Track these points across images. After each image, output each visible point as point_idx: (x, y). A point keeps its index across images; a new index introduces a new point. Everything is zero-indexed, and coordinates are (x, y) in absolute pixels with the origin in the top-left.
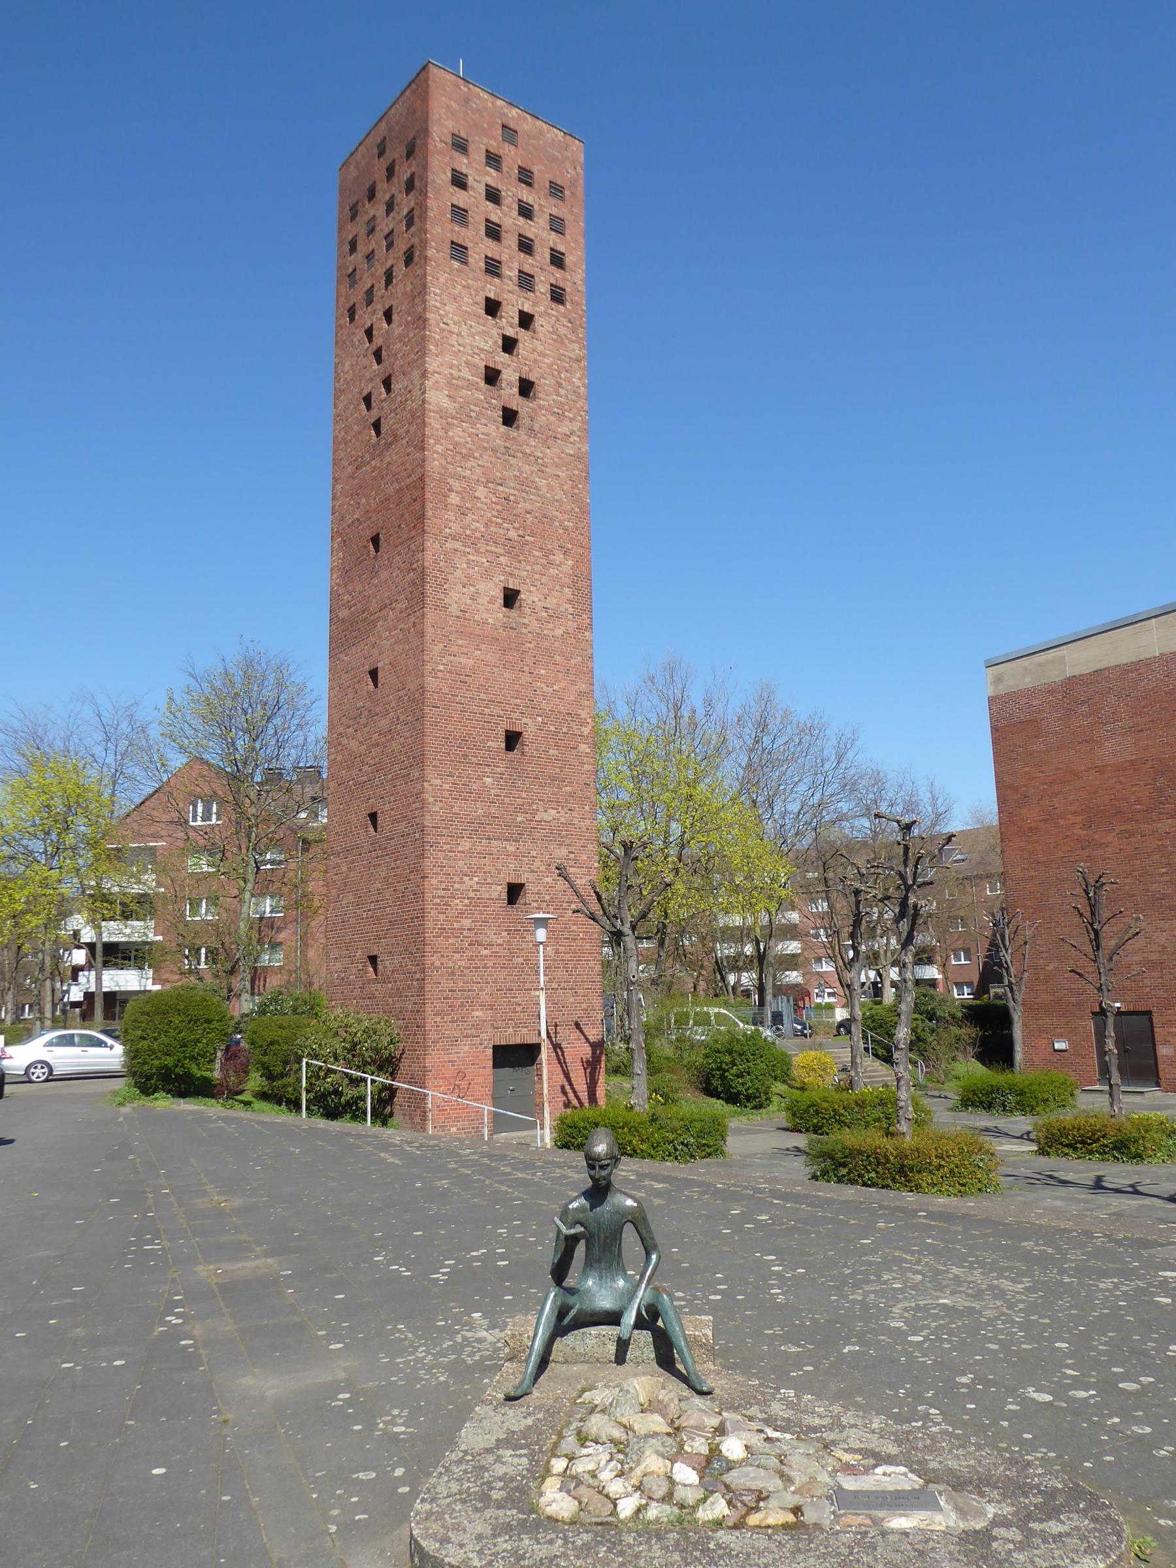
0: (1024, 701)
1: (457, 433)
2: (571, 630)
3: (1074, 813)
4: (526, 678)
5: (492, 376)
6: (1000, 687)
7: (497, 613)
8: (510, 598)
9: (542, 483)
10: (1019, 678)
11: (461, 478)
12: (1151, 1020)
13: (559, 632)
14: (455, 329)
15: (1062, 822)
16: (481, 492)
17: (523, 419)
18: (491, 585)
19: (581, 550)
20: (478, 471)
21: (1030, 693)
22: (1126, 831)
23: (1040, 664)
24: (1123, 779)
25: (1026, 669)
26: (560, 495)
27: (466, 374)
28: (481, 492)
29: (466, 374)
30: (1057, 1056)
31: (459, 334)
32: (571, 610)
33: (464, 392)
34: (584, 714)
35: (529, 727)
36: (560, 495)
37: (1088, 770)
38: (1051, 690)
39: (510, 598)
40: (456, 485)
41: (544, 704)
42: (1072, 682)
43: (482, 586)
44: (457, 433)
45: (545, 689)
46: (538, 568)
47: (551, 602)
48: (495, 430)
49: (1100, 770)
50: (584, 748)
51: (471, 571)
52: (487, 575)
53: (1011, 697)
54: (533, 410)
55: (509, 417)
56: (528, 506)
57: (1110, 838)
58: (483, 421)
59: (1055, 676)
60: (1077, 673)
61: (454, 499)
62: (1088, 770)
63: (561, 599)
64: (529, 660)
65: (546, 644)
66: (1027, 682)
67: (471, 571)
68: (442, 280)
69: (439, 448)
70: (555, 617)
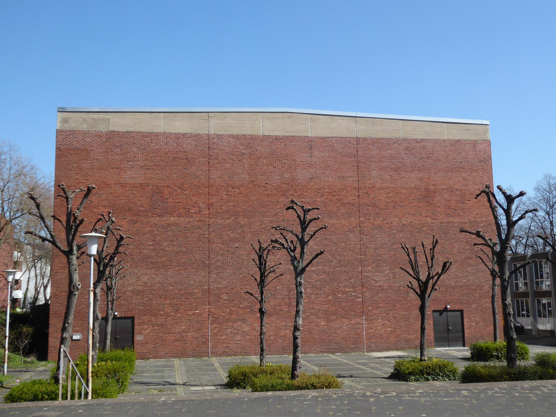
0: (80, 137)
3: (104, 207)
6: (66, 125)
10: (77, 123)
12: (133, 322)
15: (95, 210)
21: (85, 134)
22: (133, 220)
23: (93, 119)
24: (135, 192)
25: (84, 119)
30: (73, 343)
37: (116, 184)
38: (99, 135)
42: (113, 134)
49: (123, 185)
53: (73, 133)
57: (124, 223)
59: (102, 128)
60: (116, 130)
62: (116, 184)
66: (84, 127)
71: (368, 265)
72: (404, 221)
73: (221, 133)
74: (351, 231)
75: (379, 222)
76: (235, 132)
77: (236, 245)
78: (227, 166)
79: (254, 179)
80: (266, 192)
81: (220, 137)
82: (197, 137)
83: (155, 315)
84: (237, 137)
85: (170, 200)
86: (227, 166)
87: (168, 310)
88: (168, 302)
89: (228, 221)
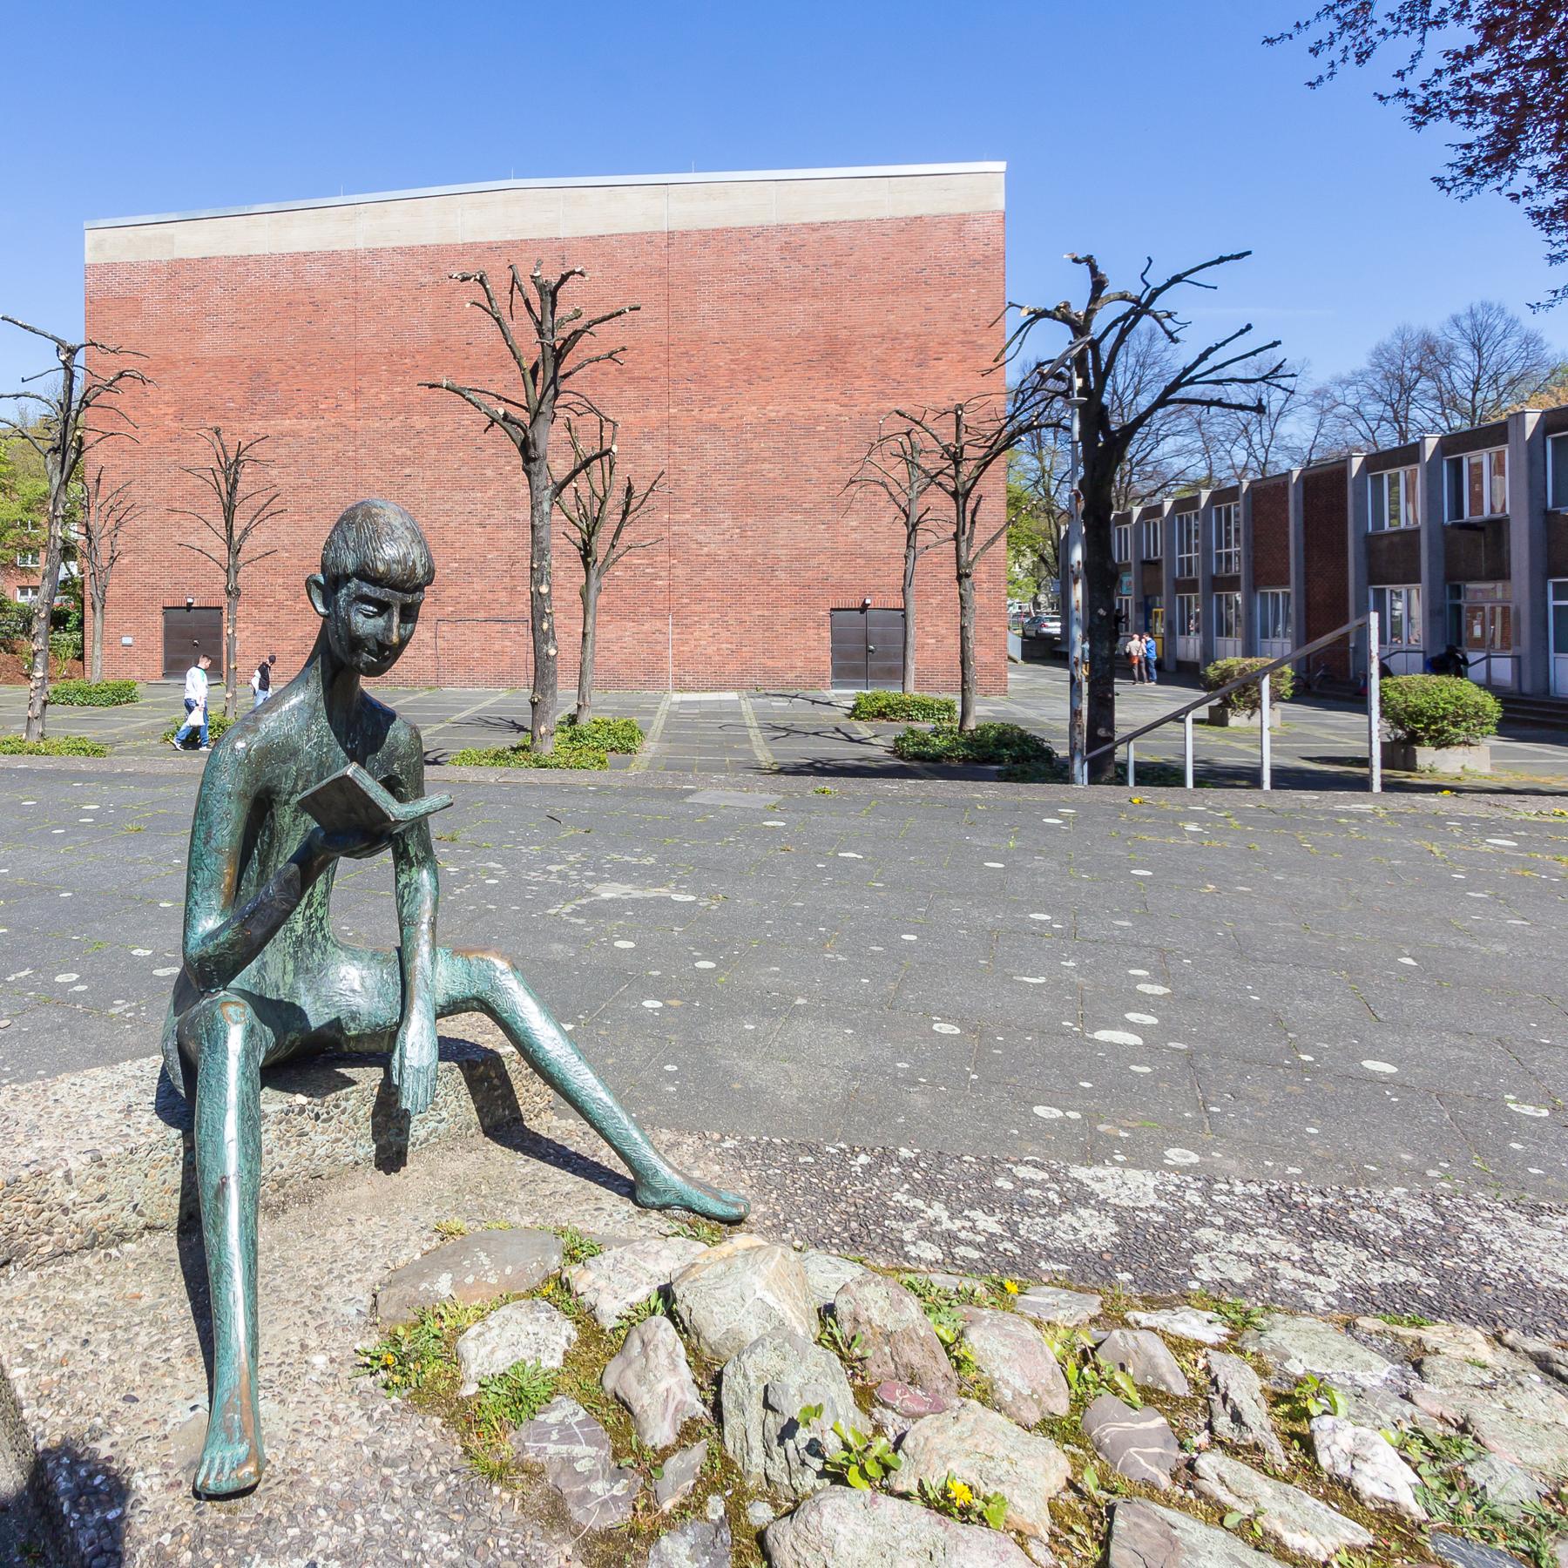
71: (683, 510)
72: (772, 411)
73: (379, 246)
74: (649, 437)
75: (711, 415)
76: (404, 243)
77: (407, 471)
78: (391, 312)
79: (443, 337)
80: (467, 362)
81: (375, 253)
82: (332, 258)
83: (257, 604)
84: (410, 252)
85: (283, 386)
86: (391, 312)
87: (281, 595)
88: (280, 581)
89: (391, 424)
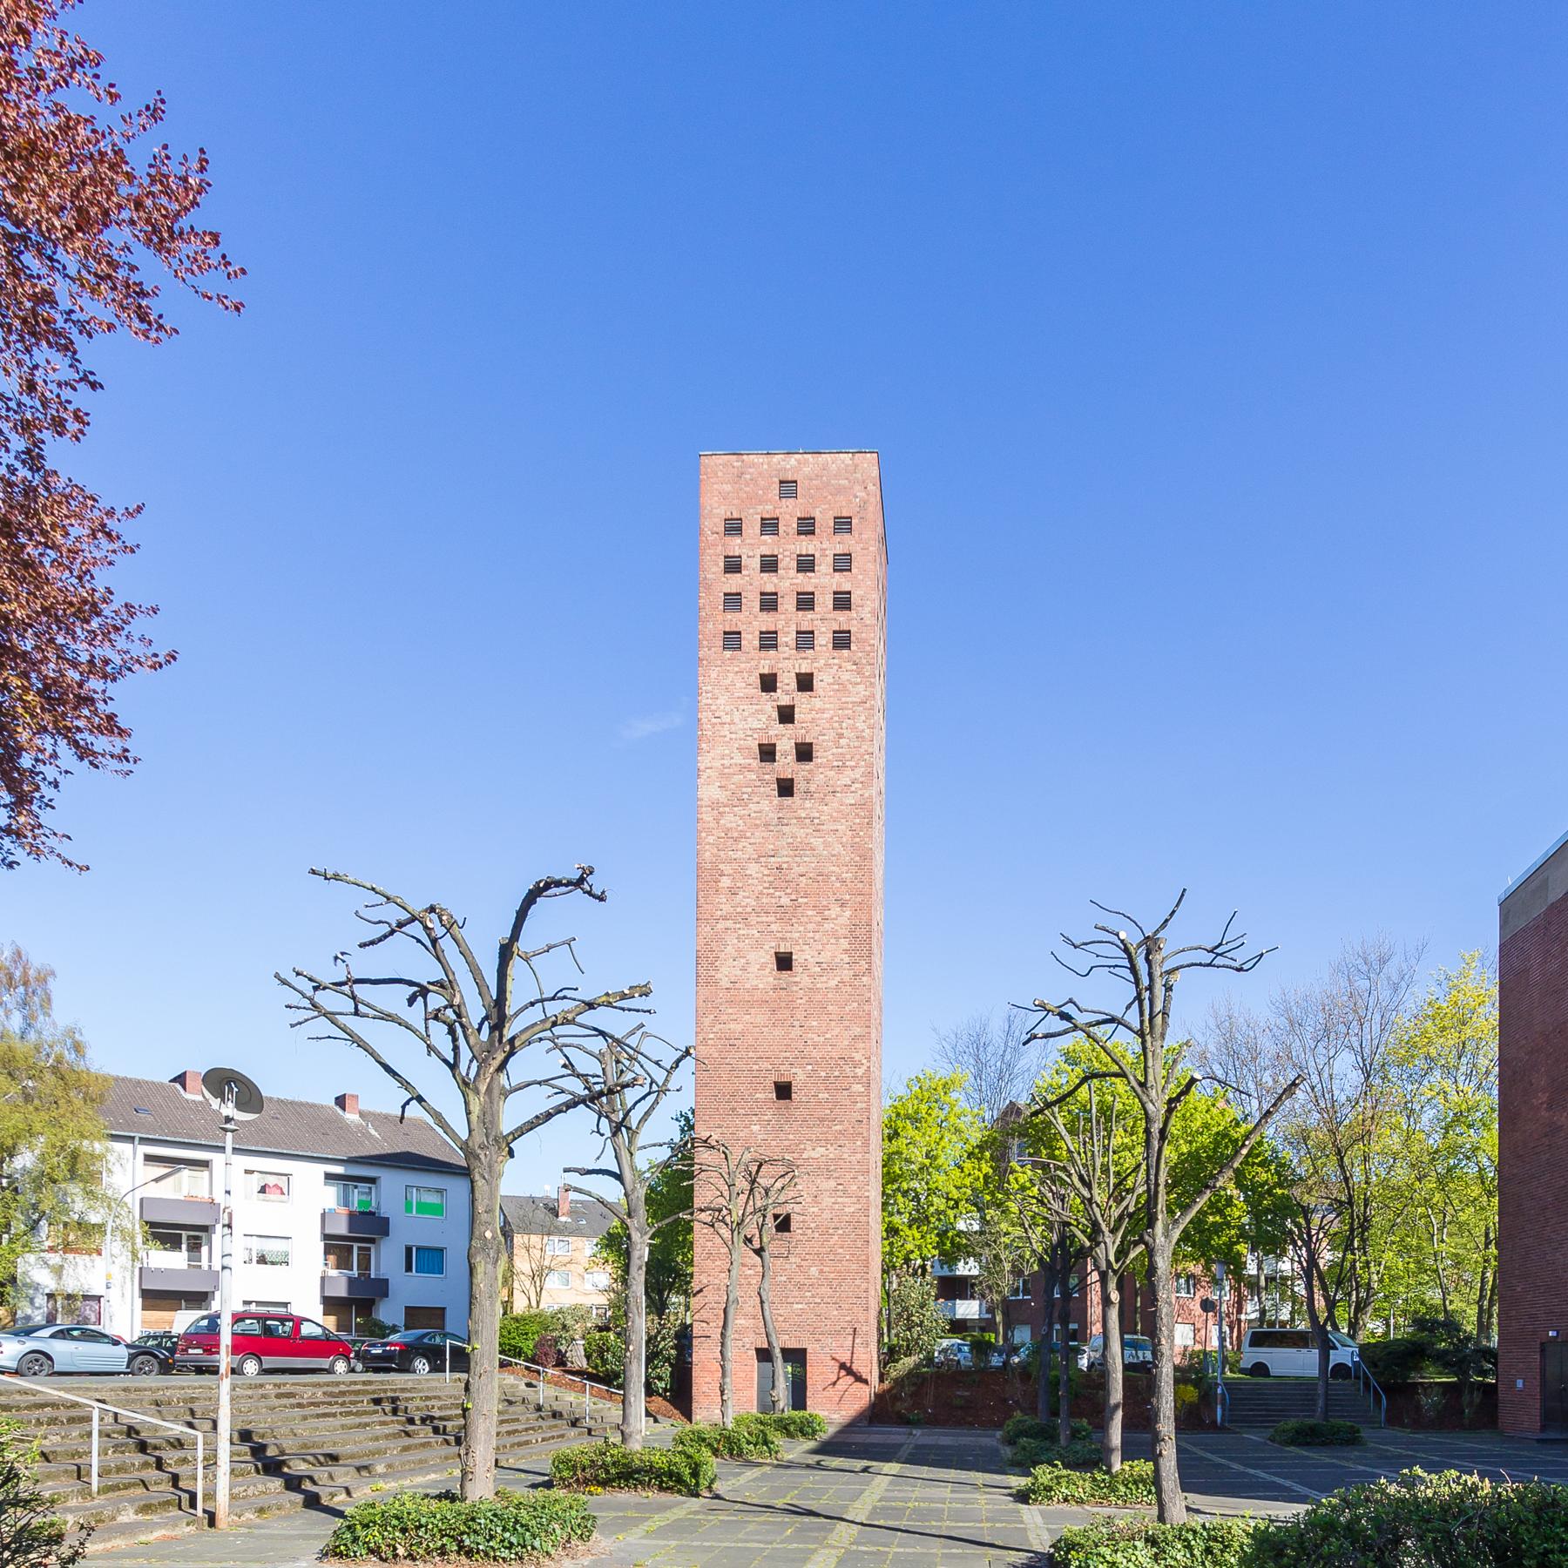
1: (729, 820)
2: (847, 979)
4: (797, 1031)
5: (767, 753)
7: (763, 974)
8: (784, 962)
9: (817, 842)
11: (731, 861)
13: (833, 983)
14: (727, 719)
16: (753, 869)
17: (799, 786)
18: (762, 953)
19: (859, 899)
20: (750, 849)
26: (838, 849)
27: (738, 759)
28: (753, 869)
29: (738, 759)
31: (732, 723)
32: (847, 959)
33: (736, 778)
34: (858, 1057)
35: (799, 1077)
36: (838, 849)
39: (784, 962)
40: (727, 868)
41: (814, 1054)
43: (752, 956)
44: (729, 820)
45: (816, 1039)
46: (811, 927)
47: (825, 957)
48: (769, 802)
50: (858, 1088)
51: (741, 945)
52: (758, 945)
54: (810, 771)
55: (786, 788)
56: (802, 870)
58: (756, 799)
61: (725, 882)
63: (836, 952)
64: (800, 1015)
65: (819, 997)
67: (741, 945)
68: (714, 675)
69: (711, 839)
70: (828, 968)
